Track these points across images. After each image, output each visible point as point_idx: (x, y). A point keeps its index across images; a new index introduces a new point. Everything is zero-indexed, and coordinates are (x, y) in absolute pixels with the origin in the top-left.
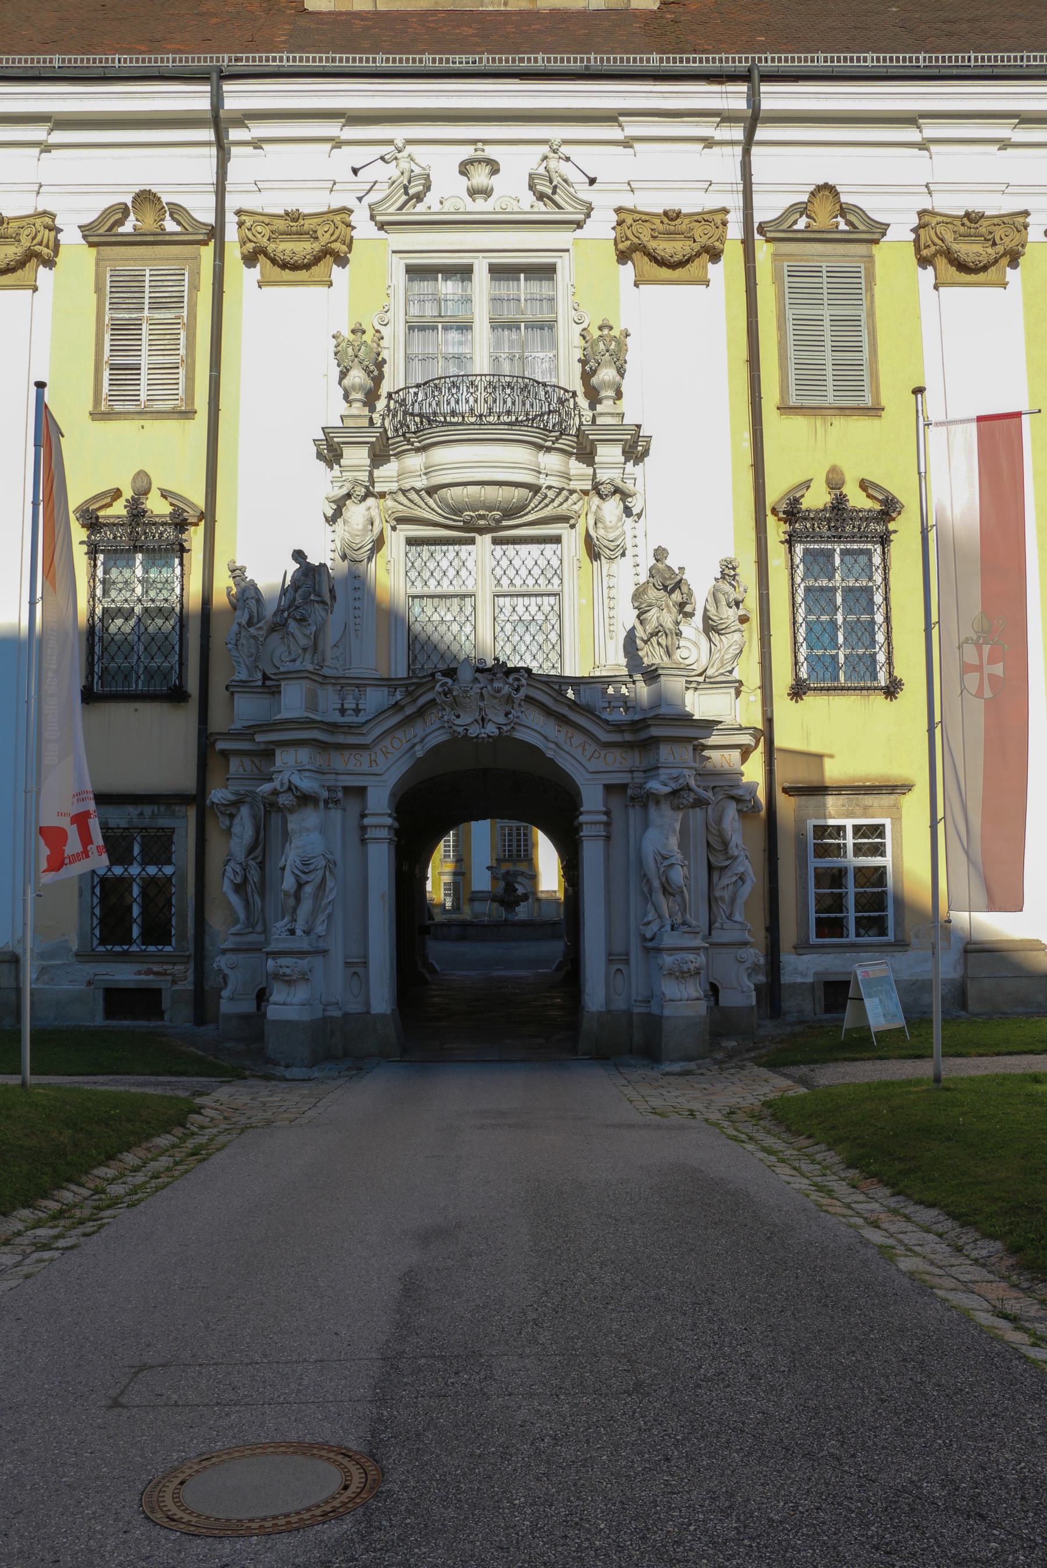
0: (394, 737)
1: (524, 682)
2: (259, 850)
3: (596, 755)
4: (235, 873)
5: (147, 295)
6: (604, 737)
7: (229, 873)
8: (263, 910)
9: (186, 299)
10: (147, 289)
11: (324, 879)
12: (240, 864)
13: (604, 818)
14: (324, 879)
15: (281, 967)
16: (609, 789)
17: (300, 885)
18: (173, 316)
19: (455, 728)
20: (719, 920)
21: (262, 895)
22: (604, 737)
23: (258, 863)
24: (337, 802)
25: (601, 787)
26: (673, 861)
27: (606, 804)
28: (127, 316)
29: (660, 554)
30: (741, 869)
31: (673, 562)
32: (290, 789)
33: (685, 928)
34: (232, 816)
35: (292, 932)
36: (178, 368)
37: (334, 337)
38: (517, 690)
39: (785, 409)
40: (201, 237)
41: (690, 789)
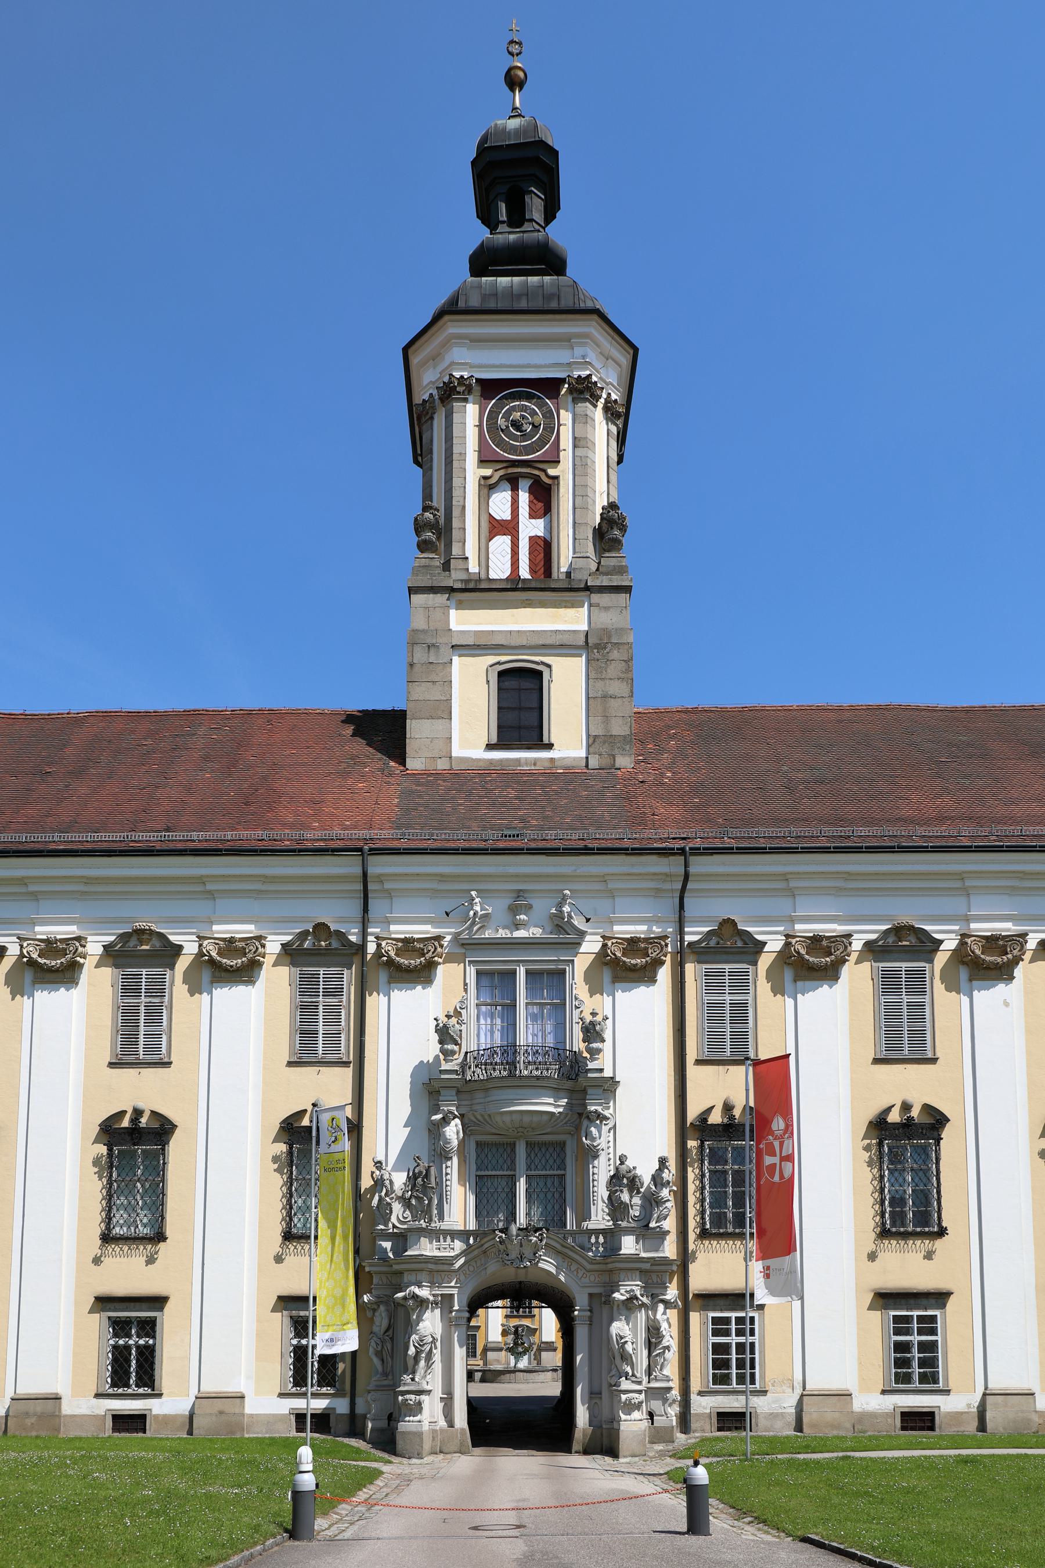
0: (470, 1265)
1: (545, 1235)
2: (391, 1330)
3: (585, 1276)
4: (377, 1344)
5: (321, 987)
6: (589, 1267)
7: (373, 1344)
8: (392, 1367)
9: (345, 990)
10: (321, 983)
11: (431, 1349)
12: (380, 1339)
13: (589, 1313)
14: (431, 1349)
15: (407, 1400)
16: (591, 1295)
17: (418, 1353)
18: (337, 1000)
19: (506, 1262)
20: (654, 1374)
21: (392, 1357)
22: (589, 1267)
23: (390, 1338)
24: (437, 1304)
25: (587, 1295)
26: (627, 1339)
27: (590, 1305)
28: (310, 1000)
29: (623, 1159)
30: (667, 1344)
31: (630, 1163)
32: (413, 1296)
33: (633, 1379)
34: (374, 1310)
35: (413, 1379)
36: (340, 1034)
37: (435, 1019)
38: (541, 1241)
39: (699, 1062)
40: (354, 951)
41: (637, 1299)
